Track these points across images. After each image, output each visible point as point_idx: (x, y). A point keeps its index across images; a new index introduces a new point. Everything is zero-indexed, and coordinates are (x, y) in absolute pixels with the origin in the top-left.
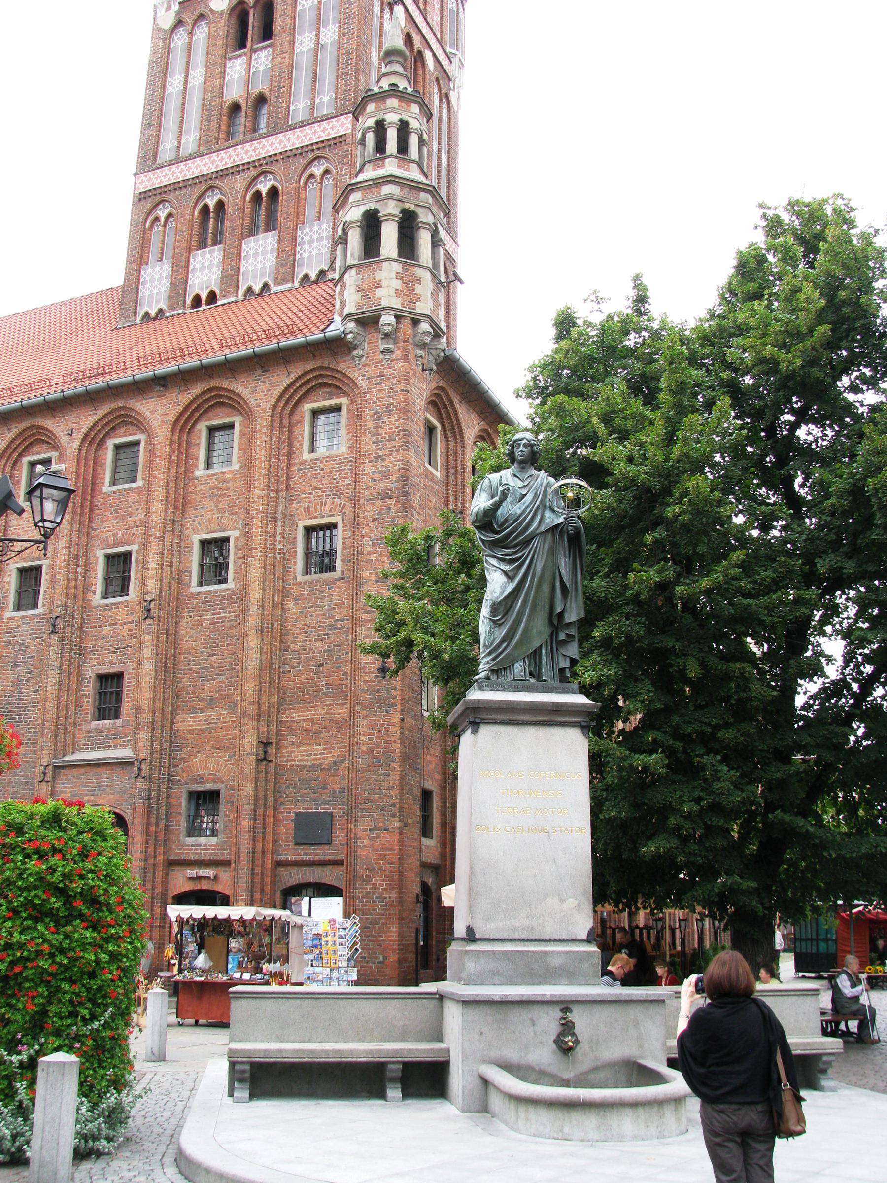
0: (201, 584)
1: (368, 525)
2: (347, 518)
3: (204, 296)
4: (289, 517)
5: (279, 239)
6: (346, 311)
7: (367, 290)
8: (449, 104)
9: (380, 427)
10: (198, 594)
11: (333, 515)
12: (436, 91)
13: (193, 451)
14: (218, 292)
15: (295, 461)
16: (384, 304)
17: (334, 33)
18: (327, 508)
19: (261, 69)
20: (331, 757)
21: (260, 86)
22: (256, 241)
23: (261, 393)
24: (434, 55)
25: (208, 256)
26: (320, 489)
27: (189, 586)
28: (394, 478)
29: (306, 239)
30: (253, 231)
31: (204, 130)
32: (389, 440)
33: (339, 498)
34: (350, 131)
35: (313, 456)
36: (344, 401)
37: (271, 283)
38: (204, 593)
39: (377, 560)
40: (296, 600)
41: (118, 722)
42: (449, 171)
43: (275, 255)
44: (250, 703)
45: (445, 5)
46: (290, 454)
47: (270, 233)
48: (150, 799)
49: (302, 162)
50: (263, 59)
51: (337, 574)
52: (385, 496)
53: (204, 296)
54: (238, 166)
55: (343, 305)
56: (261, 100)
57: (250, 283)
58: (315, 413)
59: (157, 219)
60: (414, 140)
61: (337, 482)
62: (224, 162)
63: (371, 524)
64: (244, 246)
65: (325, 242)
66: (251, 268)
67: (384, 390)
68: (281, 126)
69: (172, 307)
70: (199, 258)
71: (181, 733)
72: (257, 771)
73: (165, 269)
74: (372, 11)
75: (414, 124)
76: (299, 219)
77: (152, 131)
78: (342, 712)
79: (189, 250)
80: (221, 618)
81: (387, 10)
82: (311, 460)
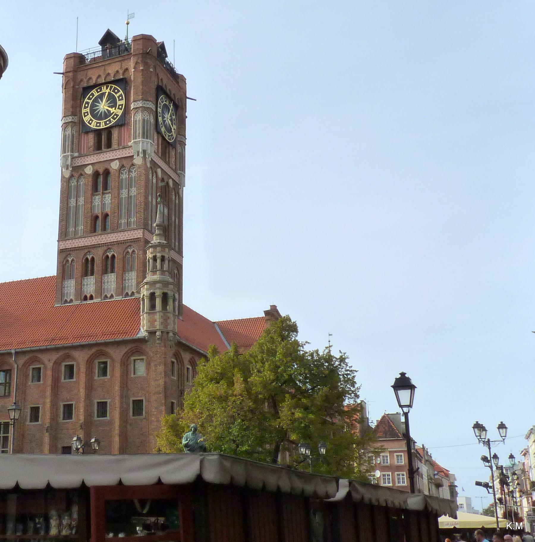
3: (88, 296)
4: (127, 397)
7: (152, 322)
16: (158, 328)
21: (108, 210)
23: (117, 354)
24: (173, 179)
29: (127, 278)
35: (135, 376)
36: (144, 357)
40: (131, 425)
49: (124, 246)
52: (159, 393)
53: (88, 296)
54: (99, 244)
56: (107, 215)
57: (106, 293)
58: (135, 360)
59: (68, 261)
68: (116, 229)
70: (86, 280)
77: (64, 223)
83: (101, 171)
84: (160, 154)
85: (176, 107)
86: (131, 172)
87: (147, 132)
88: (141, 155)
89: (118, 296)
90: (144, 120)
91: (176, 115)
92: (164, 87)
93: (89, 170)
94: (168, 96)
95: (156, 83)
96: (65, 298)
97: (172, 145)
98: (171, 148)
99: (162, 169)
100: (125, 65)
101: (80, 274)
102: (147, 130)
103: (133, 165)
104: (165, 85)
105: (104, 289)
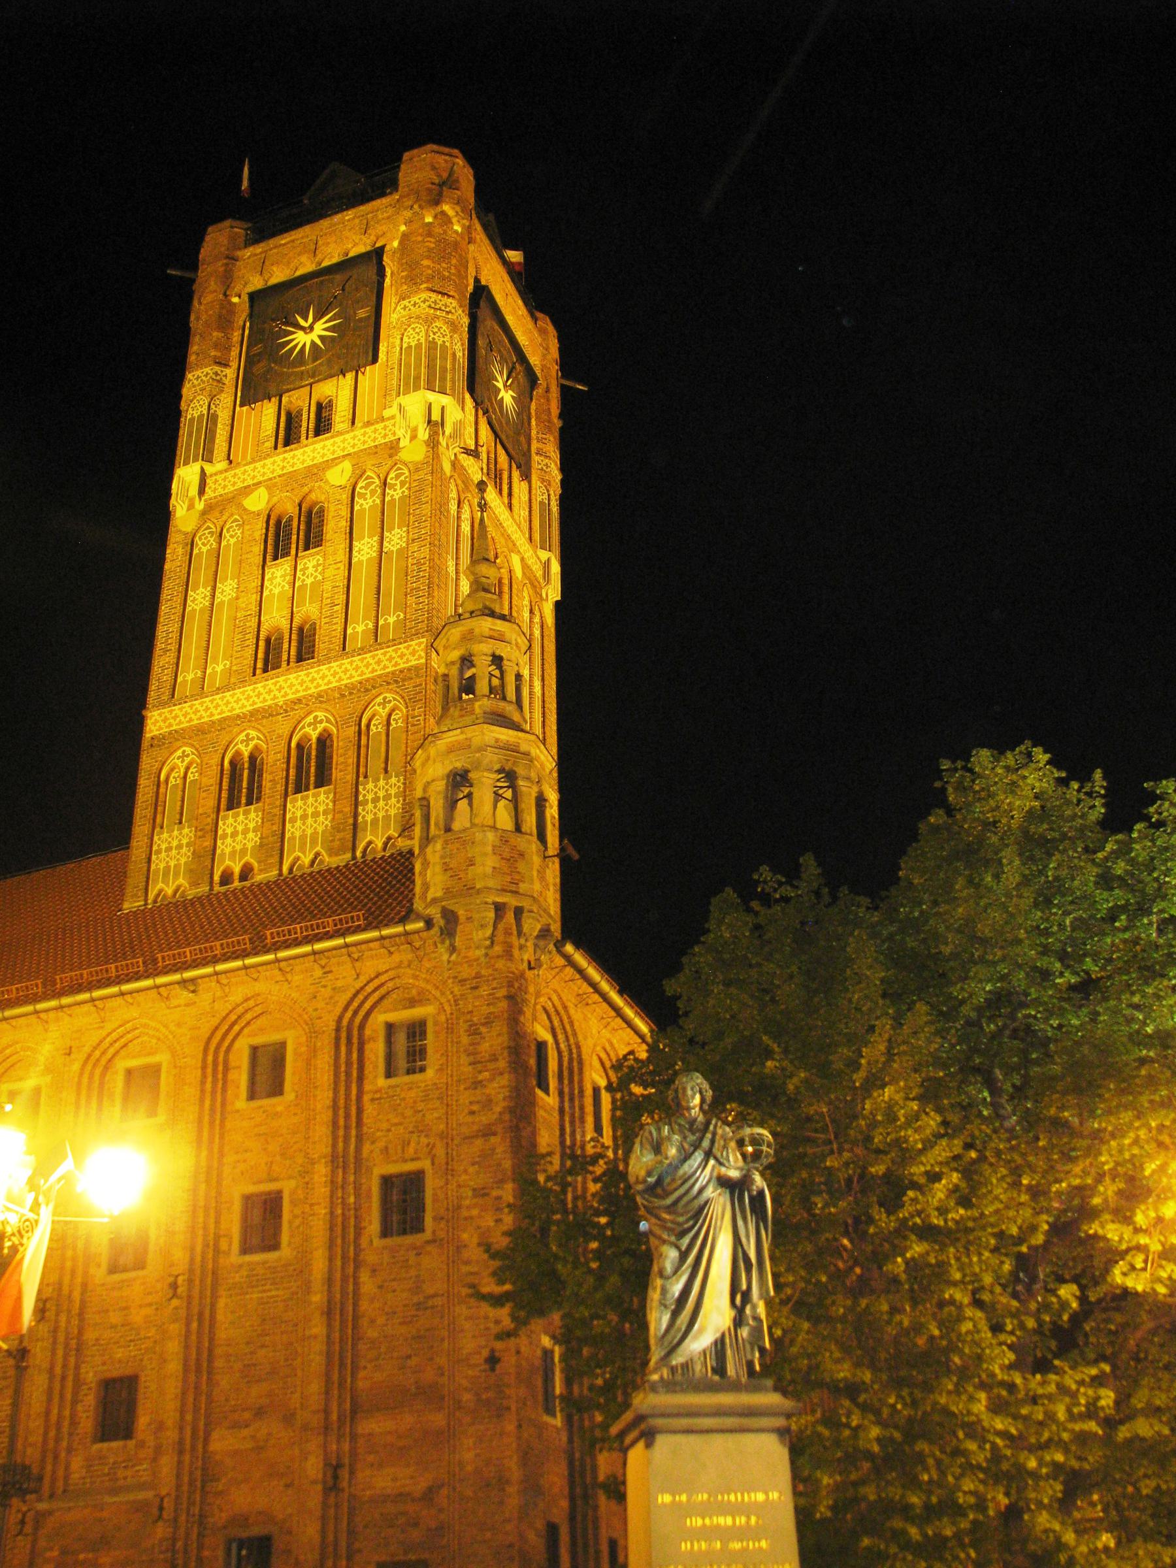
0: (244, 1251)
1: (465, 1171)
2: (436, 1161)
3: (237, 870)
5: (335, 797)
6: (430, 896)
9: (478, 1044)
10: (241, 1266)
11: (418, 1159)
13: (232, 1075)
14: (256, 865)
15: (367, 1087)
17: (401, 538)
18: (411, 1151)
19: (309, 581)
20: (422, 1485)
22: (304, 799)
25: (241, 817)
26: (401, 1124)
27: (228, 1253)
28: (498, 1109)
30: (300, 787)
32: (490, 1061)
33: (426, 1136)
34: (423, 661)
37: (323, 852)
38: (249, 1264)
39: (480, 1217)
41: (131, 1443)
42: (543, 701)
43: (330, 817)
44: (314, 1412)
45: (533, 497)
46: (361, 1079)
47: (322, 790)
48: (174, 1552)
50: (311, 570)
51: (428, 1235)
52: (487, 1132)
55: (426, 887)
61: (424, 1115)
62: (261, 698)
63: (471, 1170)
64: (289, 806)
65: (394, 800)
66: (298, 834)
67: (482, 996)
69: (195, 884)
70: (231, 820)
71: (217, 1457)
72: (325, 1505)
73: (186, 834)
74: (448, 512)
76: (360, 774)
78: (438, 1420)
80: (273, 1297)
82: (389, 1087)
86: (393, 487)
89: (337, 855)
90: (432, 345)
93: (258, 502)
96: (160, 885)
101: (212, 803)
105: (293, 838)
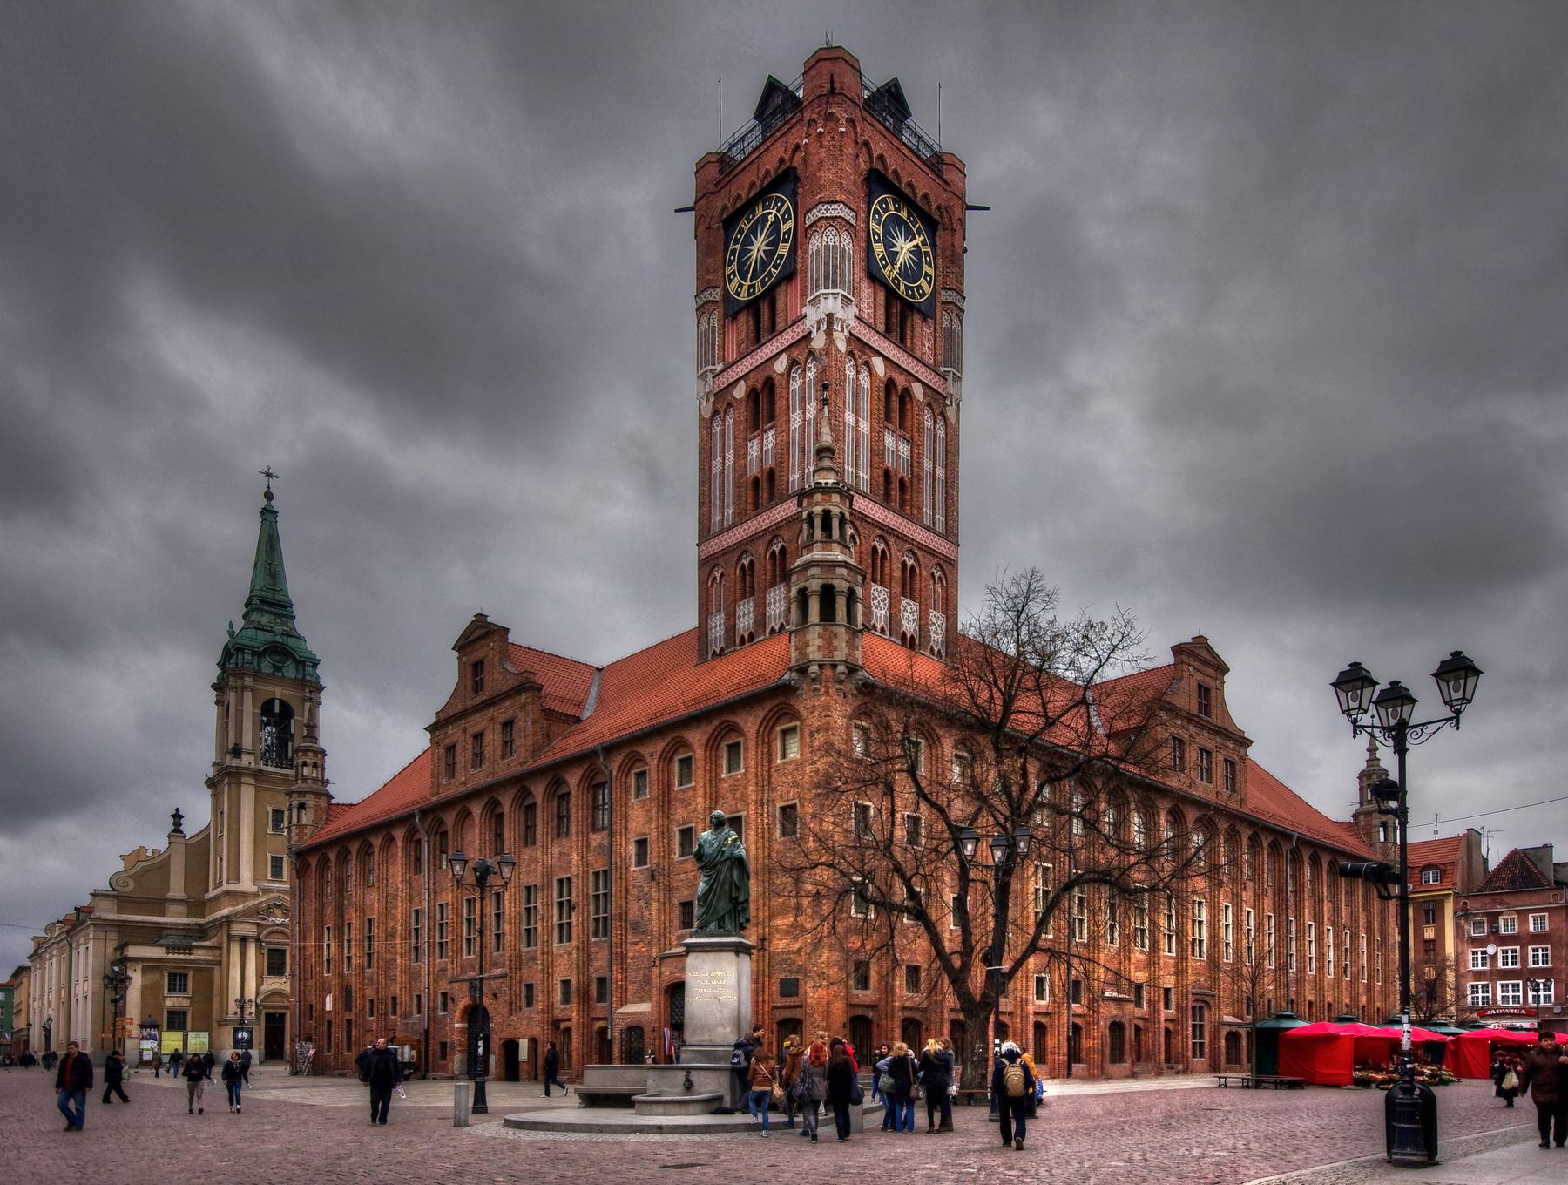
8: (945, 419)
12: (928, 415)
24: (924, 384)
30: (773, 584)
31: (737, 504)
56: (772, 472)
60: (835, 523)
75: (835, 510)
79: (735, 602)
81: (863, 369)
83: (759, 386)
84: (881, 328)
85: (931, 226)
87: (835, 273)
88: (824, 327)
91: (934, 246)
92: (891, 177)
94: (902, 198)
95: (863, 165)
97: (919, 311)
98: (917, 319)
99: (886, 358)
100: (792, 140)
102: (835, 267)
103: (811, 353)
104: (895, 172)
